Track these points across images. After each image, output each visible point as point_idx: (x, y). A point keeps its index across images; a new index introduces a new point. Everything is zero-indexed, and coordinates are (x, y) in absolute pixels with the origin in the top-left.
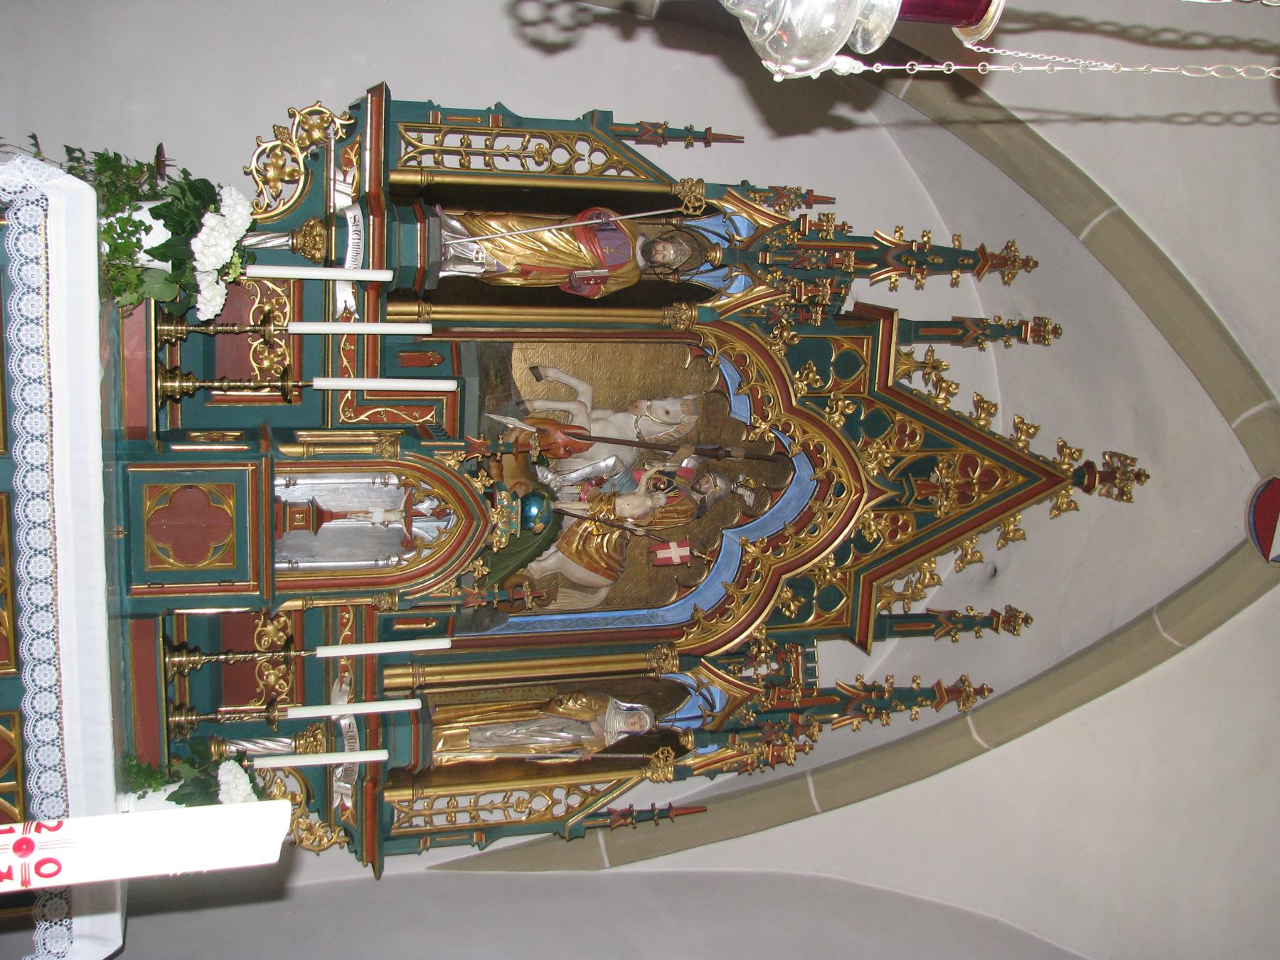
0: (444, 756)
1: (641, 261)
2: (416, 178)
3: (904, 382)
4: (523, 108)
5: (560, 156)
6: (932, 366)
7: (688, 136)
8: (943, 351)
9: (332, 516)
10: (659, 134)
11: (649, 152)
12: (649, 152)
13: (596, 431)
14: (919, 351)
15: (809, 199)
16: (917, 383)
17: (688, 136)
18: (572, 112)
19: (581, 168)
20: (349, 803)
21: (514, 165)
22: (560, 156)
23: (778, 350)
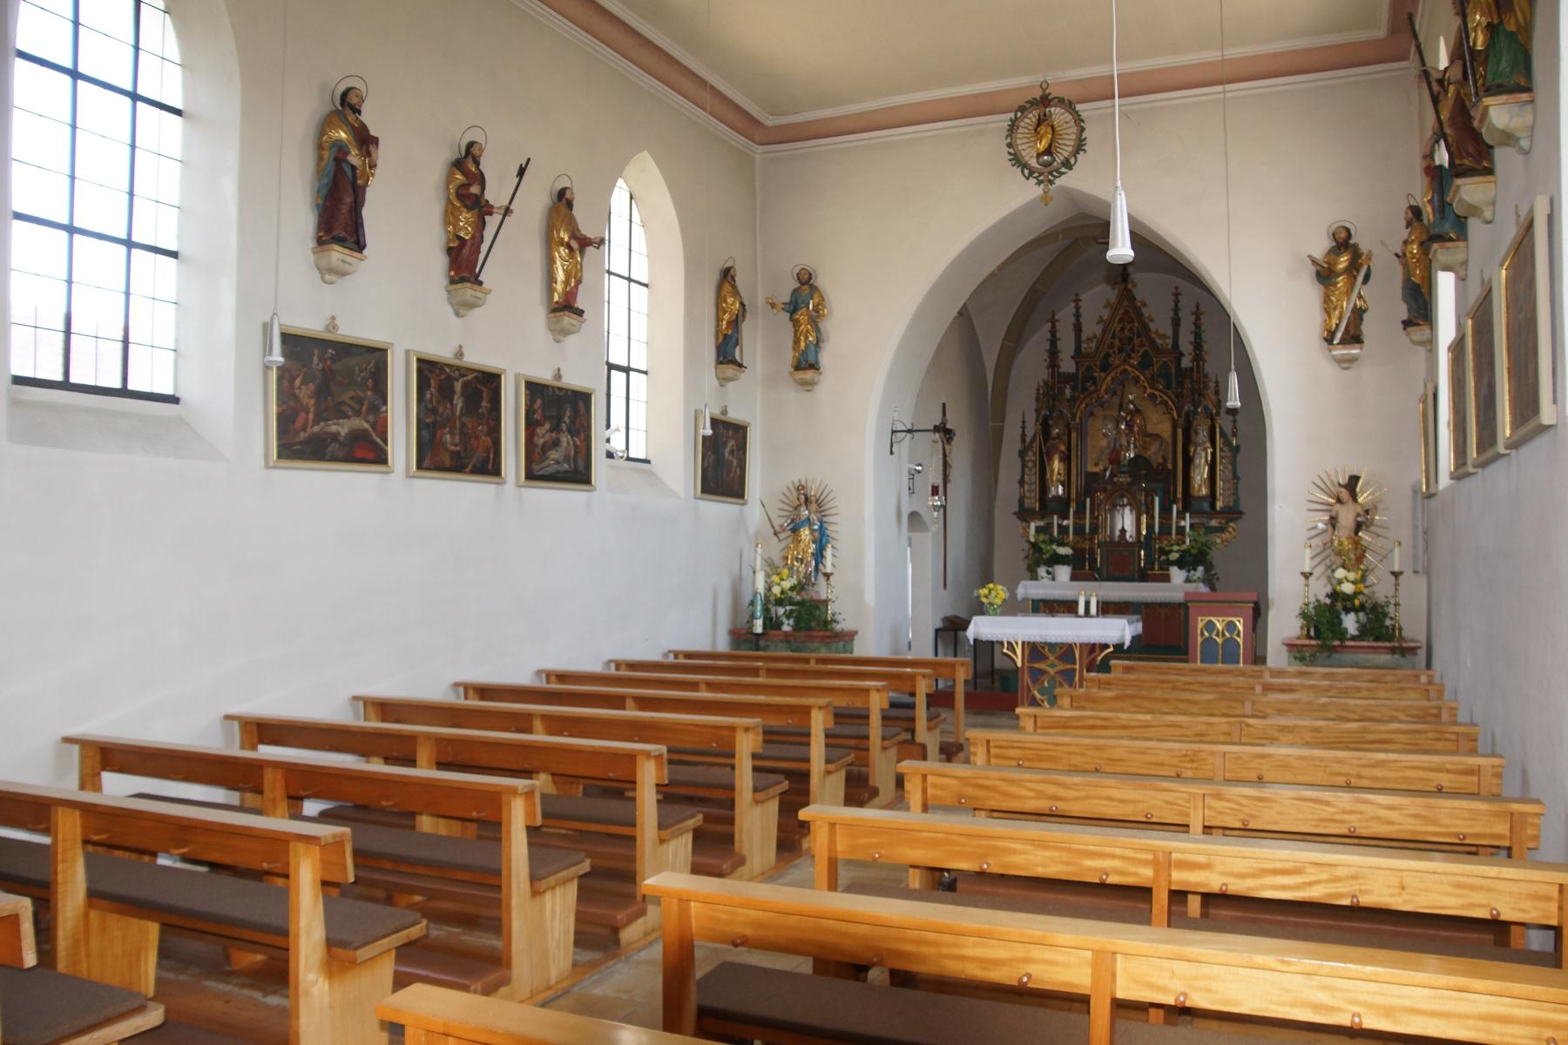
0: (1204, 491)
1: (1057, 441)
2: (1037, 504)
3: (1093, 349)
4: (1019, 477)
5: (1030, 464)
6: (1089, 340)
7: (1023, 428)
8: (1084, 338)
9: (1123, 528)
10: (1024, 436)
11: (1028, 439)
12: (1028, 439)
13: (1112, 445)
14: (1083, 345)
15: (1038, 390)
16: (1093, 345)
17: (1023, 428)
18: (1019, 461)
19: (1033, 458)
20: (1218, 521)
21: (1033, 477)
22: (1030, 464)
23: (1082, 396)
